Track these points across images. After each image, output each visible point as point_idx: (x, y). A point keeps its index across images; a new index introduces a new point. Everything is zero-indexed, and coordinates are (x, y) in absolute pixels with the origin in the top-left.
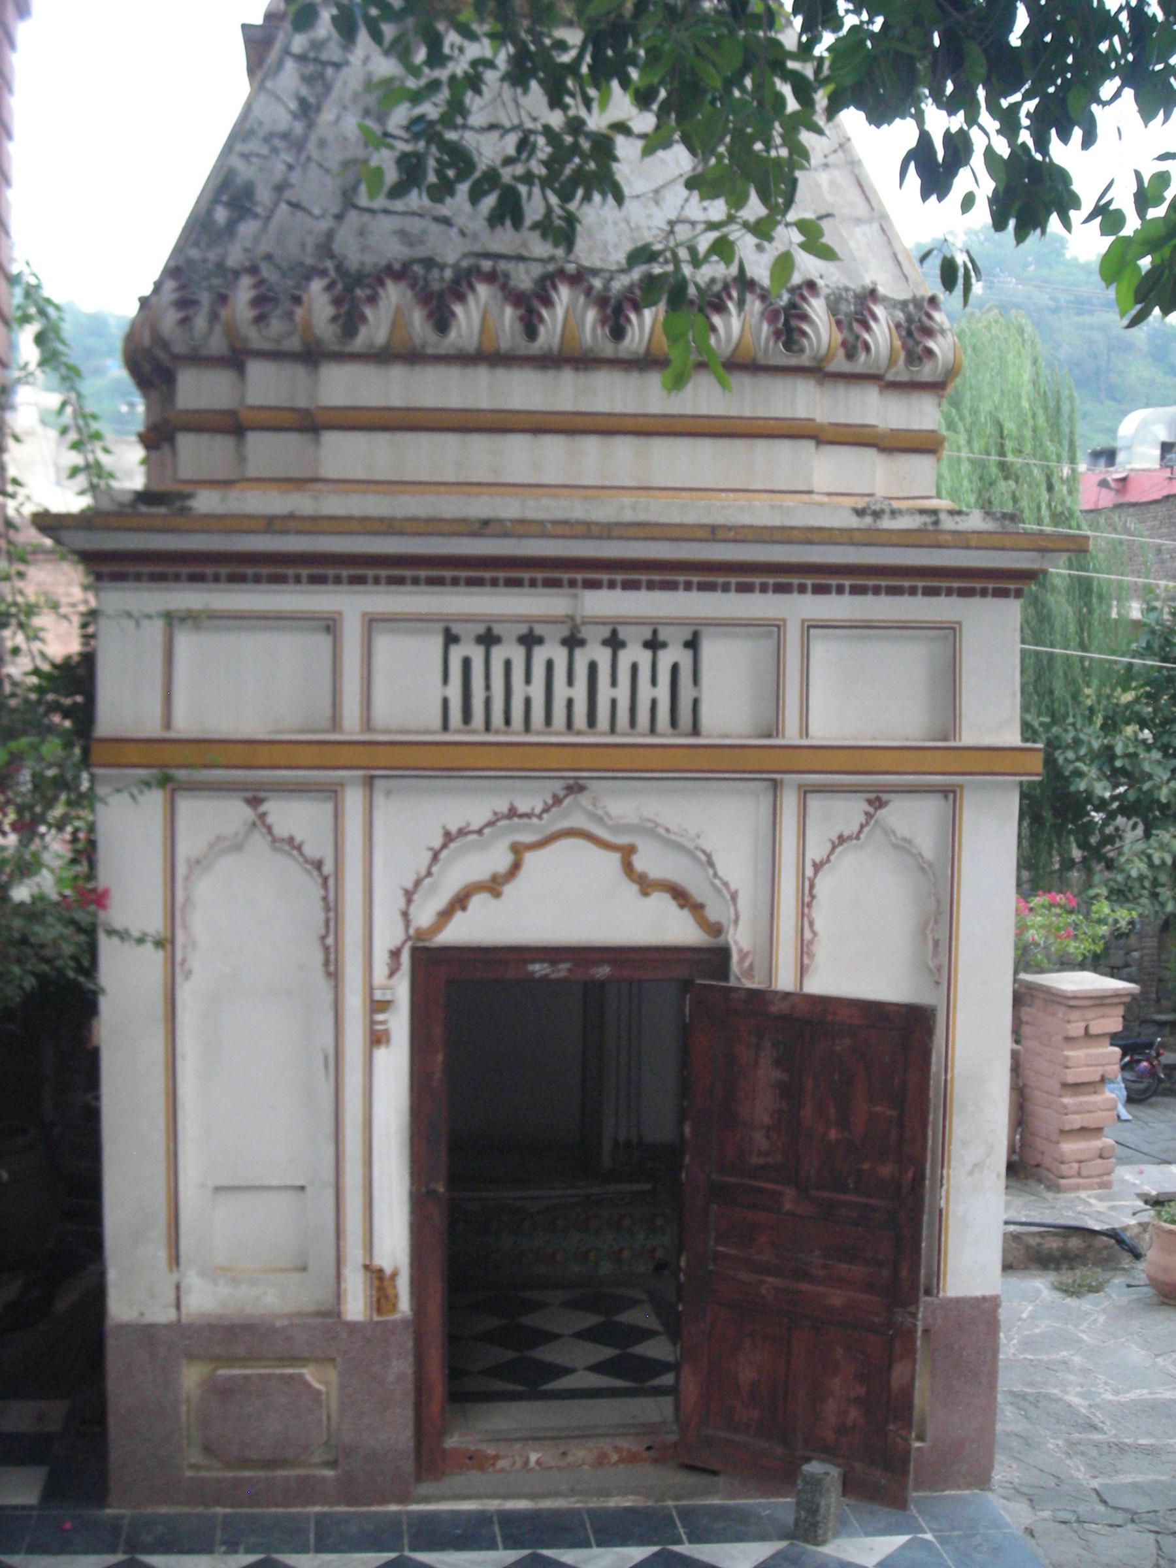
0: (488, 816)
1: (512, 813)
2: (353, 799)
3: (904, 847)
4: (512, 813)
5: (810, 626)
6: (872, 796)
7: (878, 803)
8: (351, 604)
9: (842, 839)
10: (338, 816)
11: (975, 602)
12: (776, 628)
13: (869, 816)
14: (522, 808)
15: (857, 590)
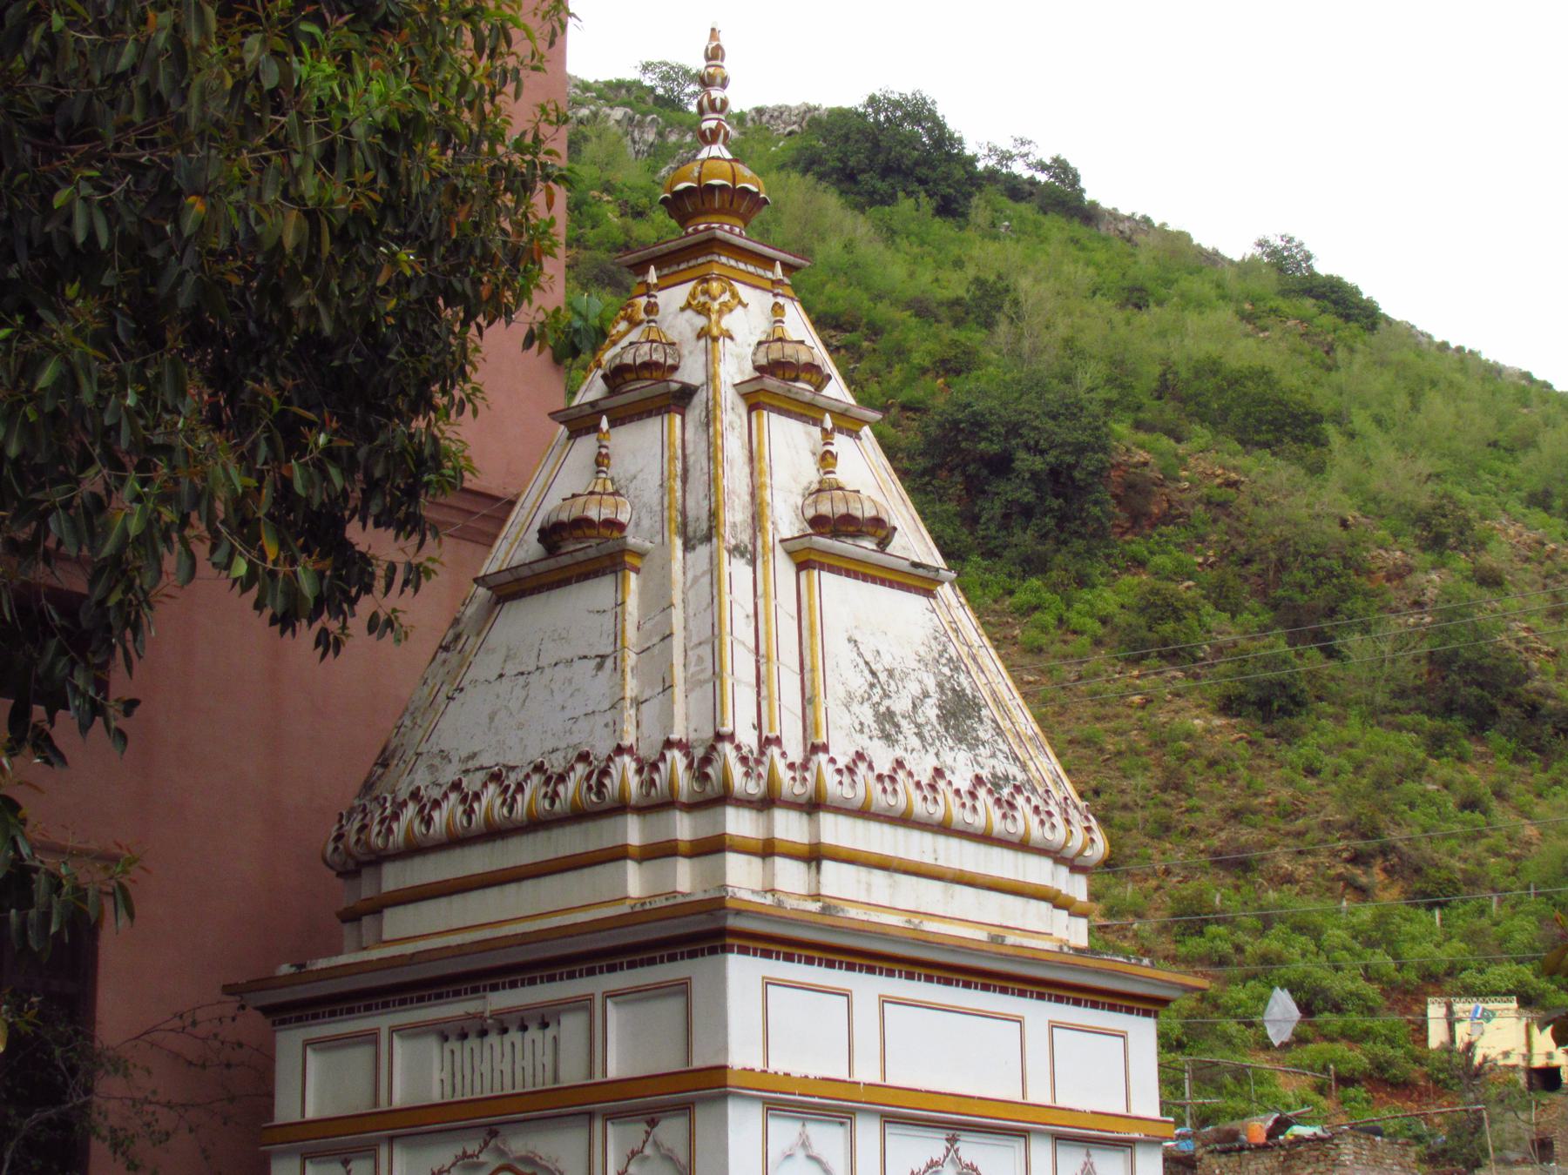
0: (453, 1159)
1: (465, 1155)
2: (383, 1153)
3: (669, 1158)
4: (465, 1155)
5: (609, 995)
6: (649, 1117)
7: (653, 1123)
8: (382, 1022)
9: (633, 1154)
10: (376, 1167)
11: (699, 960)
12: (590, 999)
13: (648, 1133)
14: (469, 1152)
15: (632, 965)
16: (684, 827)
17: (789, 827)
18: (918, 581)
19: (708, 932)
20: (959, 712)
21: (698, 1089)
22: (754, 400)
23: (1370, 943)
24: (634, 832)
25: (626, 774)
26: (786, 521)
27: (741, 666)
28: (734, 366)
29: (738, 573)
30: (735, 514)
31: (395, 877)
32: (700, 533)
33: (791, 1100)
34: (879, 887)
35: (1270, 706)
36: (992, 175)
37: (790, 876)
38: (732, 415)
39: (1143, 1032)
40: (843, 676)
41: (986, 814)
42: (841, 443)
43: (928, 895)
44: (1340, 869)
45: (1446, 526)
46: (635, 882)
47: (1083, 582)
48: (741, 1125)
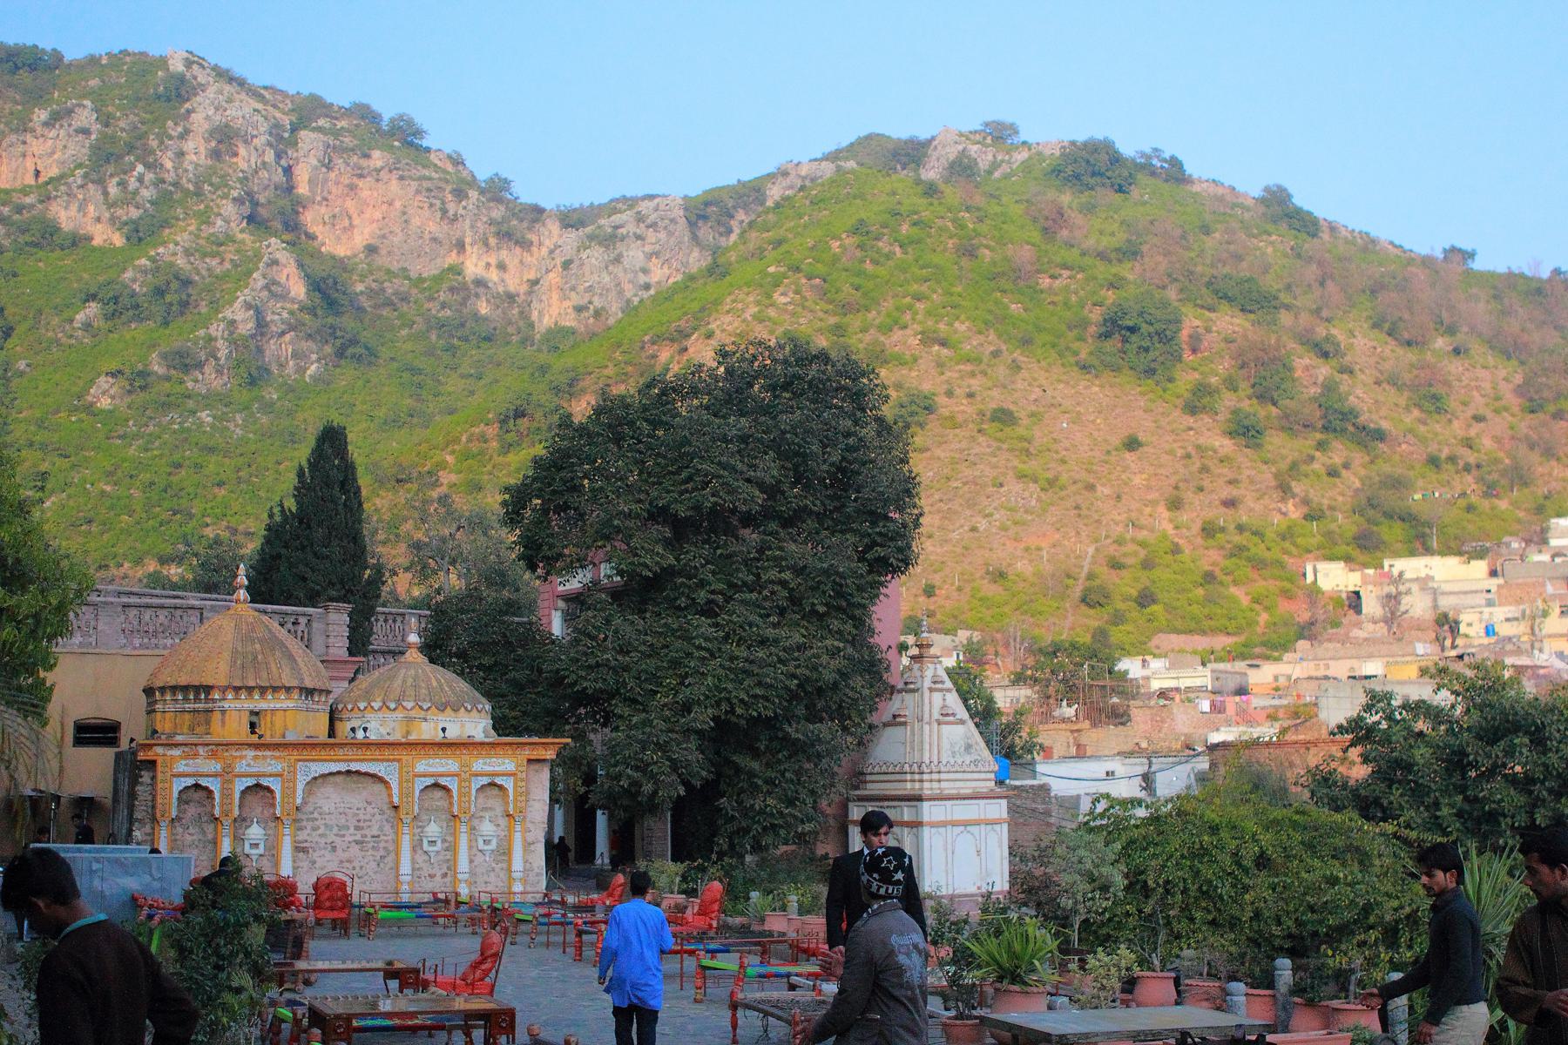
16: (917, 777)
17: (935, 776)
18: (962, 722)
19: (919, 799)
20: (968, 747)
21: (916, 825)
22: (931, 690)
23: (1284, 538)
24: (909, 777)
25: (907, 768)
26: (936, 715)
27: (927, 747)
28: (927, 683)
29: (926, 728)
30: (926, 716)
31: (868, 778)
32: (920, 720)
33: (933, 825)
34: (952, 784)
35: (1246, 432)
36: (1142, 167)
37: (935, 785)
38: (927, 694)
39: (1004, 802)
40: (945, 744)
41: (973, 768)
42: (948, 696)
43: (958, 784)
44: (1273, 506)
45: (1328, 347)
46: (909, 785)
47: (1170, 380)
48: (926, 831)
